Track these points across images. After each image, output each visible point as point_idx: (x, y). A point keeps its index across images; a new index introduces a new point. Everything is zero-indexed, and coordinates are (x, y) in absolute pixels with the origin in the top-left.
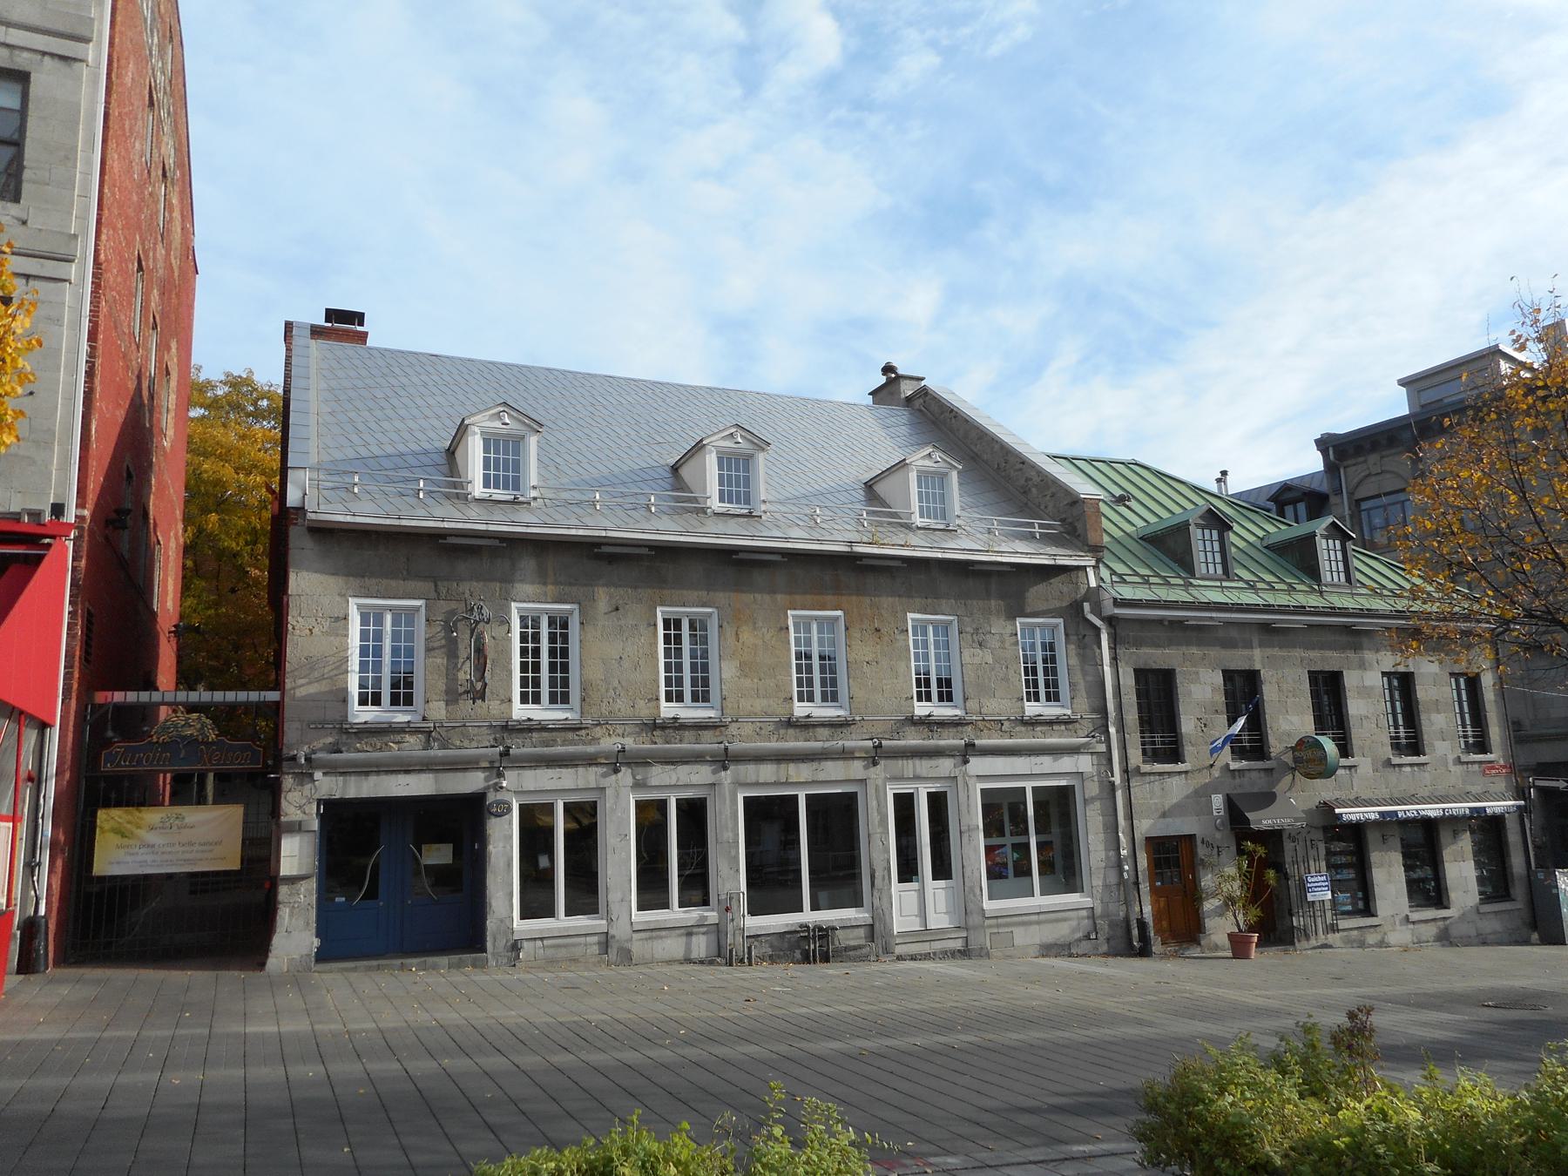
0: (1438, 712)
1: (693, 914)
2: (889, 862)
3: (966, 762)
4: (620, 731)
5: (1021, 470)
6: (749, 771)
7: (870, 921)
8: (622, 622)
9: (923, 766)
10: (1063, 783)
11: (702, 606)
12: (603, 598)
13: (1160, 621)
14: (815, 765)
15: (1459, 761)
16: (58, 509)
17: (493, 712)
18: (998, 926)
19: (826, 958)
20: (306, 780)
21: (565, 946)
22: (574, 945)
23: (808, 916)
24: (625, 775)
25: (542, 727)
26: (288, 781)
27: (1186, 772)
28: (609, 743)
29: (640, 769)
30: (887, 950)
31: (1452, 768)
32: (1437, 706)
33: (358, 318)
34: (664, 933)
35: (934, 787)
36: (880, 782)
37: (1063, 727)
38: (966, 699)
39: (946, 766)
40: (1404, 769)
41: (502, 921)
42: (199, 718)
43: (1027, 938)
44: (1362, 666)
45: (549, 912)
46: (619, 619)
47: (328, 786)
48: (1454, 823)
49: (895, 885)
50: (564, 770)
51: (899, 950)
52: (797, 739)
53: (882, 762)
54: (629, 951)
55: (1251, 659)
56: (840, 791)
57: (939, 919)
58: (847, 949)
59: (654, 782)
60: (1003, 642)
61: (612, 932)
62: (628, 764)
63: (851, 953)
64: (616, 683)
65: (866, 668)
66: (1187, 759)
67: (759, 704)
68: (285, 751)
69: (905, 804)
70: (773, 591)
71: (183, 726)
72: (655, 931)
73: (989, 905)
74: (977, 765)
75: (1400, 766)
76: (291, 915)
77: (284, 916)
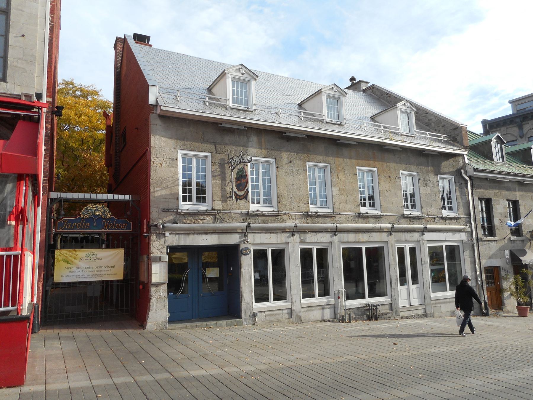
1: (324, 300)
2: (397, 277)
3: (423, 234)
4: (294, 217)
5: (425, 116)
7: (391, 302)
8: (293, 168)
9: (408, 236)
10: (455, 244)
11: (324, 163)
12: (285, 156)
13: (486, 179)
14: (369, 234)
16: (39, 96)
17: (241, 207)
18: (436, 304)
19: (376, 319)
20: (162, 236)
21: (274, 315)
22: (278, 314)
23: (368, 300)
24: (297, 237)
25: (263, 215)
26: (153, 237)
27: (496, 241)
28: (290, 224)
29: (302, 235)
30: (397, 315)
33: (148, 38)
34: (313, 308)
35: (412, 245)
36: (393, 242)
37: (456, 221)
38: (422, 208)
39: (416, 236)
41: (248, 304)
42: (103, 207)
46: (292, 167)
47: (172, 240)
49: (400, 287)
50: (272, 234)
51: (402, 314)
52: (362, 223)
53: (394, 234)
54: (300, 317)
55: (515, 195)
56: (377, 246)
57: (415, 302)
58: (383, 314)
59: (308, 240)
60: (434, 184)
61: (293, 308)
62: (298, 232)
63: (385, 316)
64: (291, 196)
65: (386, 193)
66: (497, 235)
67: (348, 207)
68: (151, 222)
69: (401, 251)
71: (95, 210)
72: (310, 307)
73: (434, 295)
74: (428, 236)
76: (157, 302)
77: (153, 302)
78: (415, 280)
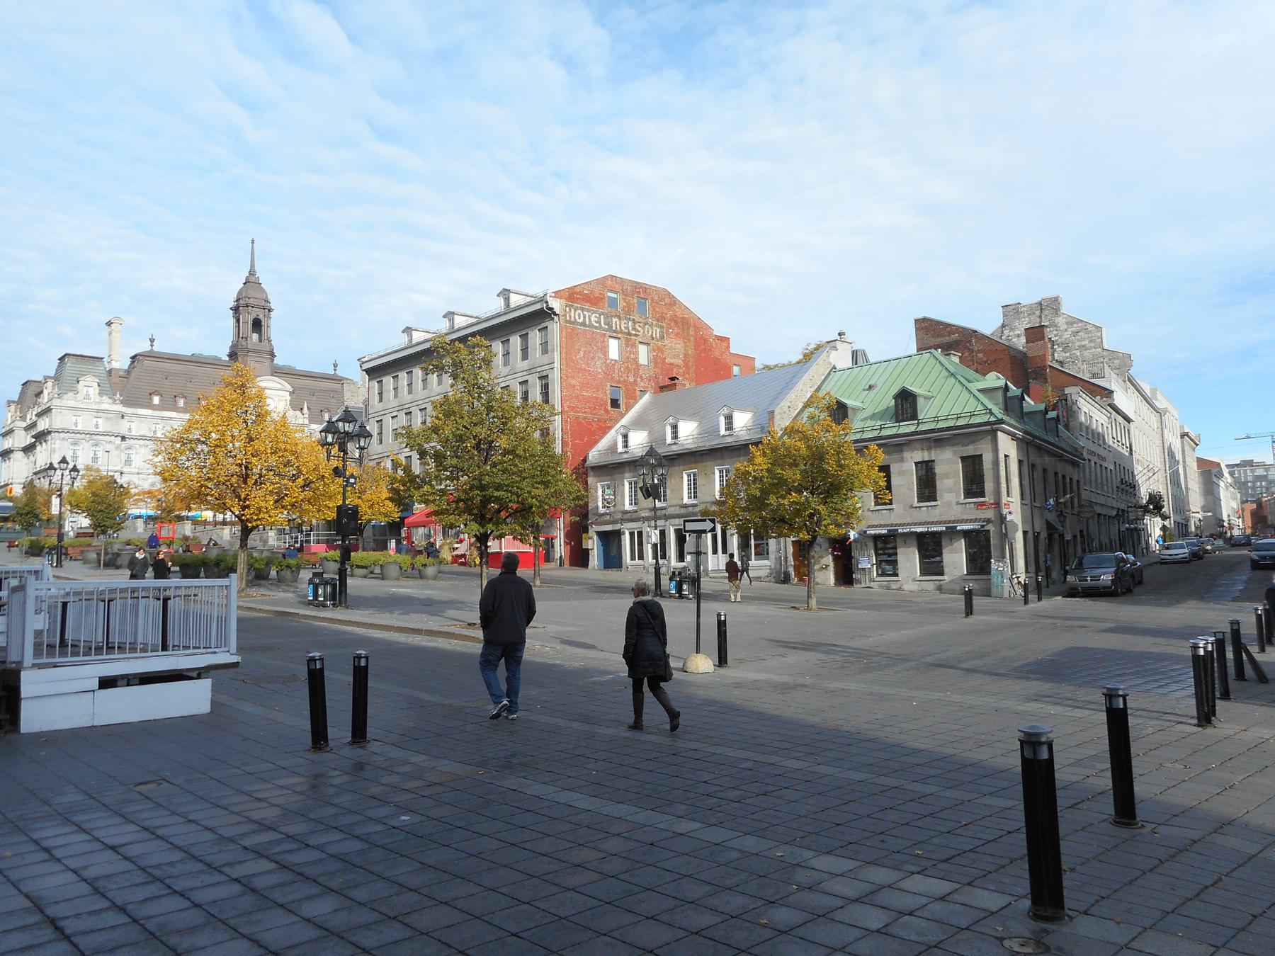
0: (948, 478)
6: (673, 521)
15: (958, 503)
26: (590, 527)
30: (707, 575)
31: (955, 507)
32: (947, 476)
40: (922, 509)
44: (902, 460)
48: (952, 533)
51: (711, 575)
70: (679, 465)
75: (920, 507)
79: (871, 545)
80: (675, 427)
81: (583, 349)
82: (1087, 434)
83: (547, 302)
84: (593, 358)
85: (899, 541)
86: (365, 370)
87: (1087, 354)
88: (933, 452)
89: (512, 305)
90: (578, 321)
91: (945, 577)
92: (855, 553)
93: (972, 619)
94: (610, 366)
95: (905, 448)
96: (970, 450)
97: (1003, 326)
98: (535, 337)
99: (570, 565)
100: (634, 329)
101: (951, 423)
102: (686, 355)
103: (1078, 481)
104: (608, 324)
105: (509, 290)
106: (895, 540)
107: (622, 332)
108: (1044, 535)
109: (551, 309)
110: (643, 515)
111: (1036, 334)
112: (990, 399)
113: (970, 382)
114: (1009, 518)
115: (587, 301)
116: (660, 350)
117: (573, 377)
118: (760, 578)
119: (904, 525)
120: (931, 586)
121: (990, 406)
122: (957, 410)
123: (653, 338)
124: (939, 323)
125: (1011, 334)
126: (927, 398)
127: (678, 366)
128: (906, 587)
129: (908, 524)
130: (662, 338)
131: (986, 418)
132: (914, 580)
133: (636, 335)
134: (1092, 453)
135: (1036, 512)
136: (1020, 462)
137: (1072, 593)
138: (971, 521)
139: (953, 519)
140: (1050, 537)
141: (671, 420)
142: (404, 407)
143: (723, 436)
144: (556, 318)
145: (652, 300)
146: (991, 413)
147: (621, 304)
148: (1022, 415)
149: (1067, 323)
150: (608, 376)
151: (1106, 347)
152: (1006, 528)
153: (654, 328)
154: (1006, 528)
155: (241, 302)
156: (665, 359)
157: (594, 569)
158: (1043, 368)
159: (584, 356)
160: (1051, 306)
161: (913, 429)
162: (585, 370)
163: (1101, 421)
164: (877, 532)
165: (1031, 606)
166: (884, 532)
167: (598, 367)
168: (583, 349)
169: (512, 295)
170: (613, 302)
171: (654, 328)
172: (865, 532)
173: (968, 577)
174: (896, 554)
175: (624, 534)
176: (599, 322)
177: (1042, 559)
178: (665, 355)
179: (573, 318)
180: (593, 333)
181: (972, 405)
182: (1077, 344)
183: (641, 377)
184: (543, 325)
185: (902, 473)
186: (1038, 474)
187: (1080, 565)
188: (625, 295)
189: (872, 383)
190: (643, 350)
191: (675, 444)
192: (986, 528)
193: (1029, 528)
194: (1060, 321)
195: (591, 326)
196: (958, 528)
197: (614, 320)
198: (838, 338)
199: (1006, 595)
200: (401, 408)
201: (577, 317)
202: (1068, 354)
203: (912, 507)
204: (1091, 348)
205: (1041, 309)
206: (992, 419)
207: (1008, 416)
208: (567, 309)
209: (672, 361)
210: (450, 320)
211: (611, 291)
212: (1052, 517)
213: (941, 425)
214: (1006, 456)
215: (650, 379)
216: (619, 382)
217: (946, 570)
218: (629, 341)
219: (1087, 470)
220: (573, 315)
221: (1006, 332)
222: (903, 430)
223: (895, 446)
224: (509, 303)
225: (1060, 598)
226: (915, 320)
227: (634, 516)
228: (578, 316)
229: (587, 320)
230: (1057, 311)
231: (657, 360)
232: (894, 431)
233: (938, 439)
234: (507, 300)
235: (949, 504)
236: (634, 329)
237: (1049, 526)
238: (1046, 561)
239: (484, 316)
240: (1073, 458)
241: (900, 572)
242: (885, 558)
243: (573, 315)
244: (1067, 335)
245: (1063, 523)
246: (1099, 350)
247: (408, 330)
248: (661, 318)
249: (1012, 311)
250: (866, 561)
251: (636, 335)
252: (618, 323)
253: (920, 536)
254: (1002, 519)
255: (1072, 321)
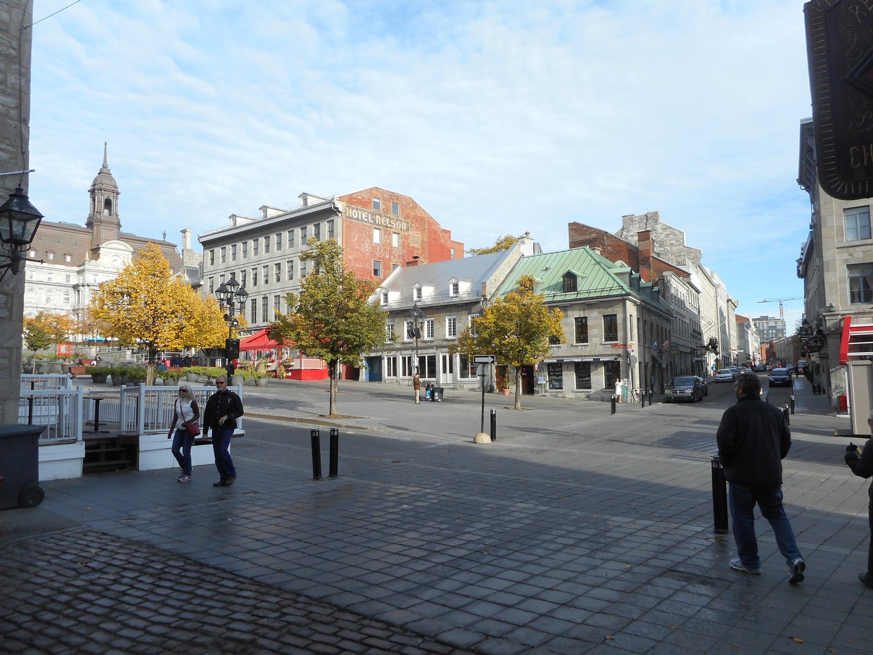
0: (595, 328)
12: (397, 320)
15: (601, 344)
31: (599, 346)
32: (594, 327)
43: (466, 387)
45: (405, 375)
48: (597, 363)
72: (403, 380)
78: (451, 371)
79: (546, 369)
80: (419, 290)
81: (357, 236)
82: (675, 300)
83: (334, 204)
84: (363, 242)
85: (564, 367)
86: (202, 242)
87: (674, 249)
88: (586, 312)
89: (309, 204)
90: (354, 217)
91: (592, 390)
92: (536, 374)
93: (615, 415)
94: (374, 247)
95: (569, 309)
96: (609, 311)
97: (623, 229)
98: (325, 226)
99: (347, 378)
100: (390, 223)
101: (598, 294)
102: (423, 242)
103: (669, 331)
104: (373, 220)
105: (307, 194)
106: (561, 367)
107: (382, 225)
108: (650, 364)
109: (337, 208)
110: (397, 347)
111: (644, 236)
112: (622, 280)
113: (609, 268)
114: (632, 354)
115: (360, 204)
116: (406, 238)
117: (350, 254)
118: (474, 389)
119: (567, 357)
120: (583, 395)
121: (622, 284)
122: (601, 286)
123: (402, 230)
124: (584, 226)
125: (628, 234)
126: (583, 278)
127: (418, 249)
128: (567, 396)
129: (570, 357)
130: (408, 230)
131: (619, 292)
132: (573, 391)
133: (391, 228)
134: (678, 313)
135: (646, 350)
136: (638, 319)
137: (668, 401)
138: (609, 355)
139: (597, 354)
140: (653, 365)
141: (417, 286)
142: (229, 269)
143: (451, 297)
144: (340, 215)
145: (402, 204)
146: (623, 289)
147: (382, 206)
148: (640, 290)
149: (662, 229)
150: (373, 254)
151: (686, 245)
152: (630, 360)
153: (403, 223)
154: (630, 360)
155: (96, 186)
156: (409, 244)
157: (362, 381)
158: (648, 258)
159: (358, 241)
160: (652, 217)
161: (574, 297)
162: (358, 249)
163: (683, 293)
164: (550, 361)
165: (646, 408)
166: (554, 361)
167: (366, 248)
168: (357, 236)
169: (309, 197)
170: (376, 206)
171: (403, 223)
172: (543, 361)
173: (606, 390)
174: (561, 375)
175: (384, 359)
176: (367, 218)
177: (649, 379)
178: (409, 241)
179: (351, 215)
180: (364, 225)
181: (611, 283)
182: (668, 242)
183: (394, 255)
184: (330, 219)
185: (567, 324)
186: (648, 327)
187: (672, 384)
188: (385, 201)
189: (547, 266)
190: (395, 237)
191: (419, 301)
192: (618, 360)
193: (642, 361)
194: (658, 227)
195: (362, 220)
196: (601, 360)
197: (378, 217)
198: (525, 236)
199: (629, 401)
200: (227, 269)
201: (353, 215)
202: (663, 249)
203: (572, 346)
204: (676, 245)
205: (647, 219)
206: (624, 292)
207: (632, 290)
208: (347, 209)
209: (414, 245)
210: (264, 211)
211: (375, 198)
212: (655, 354)
213: (592, 295)
214: (631, 316)
215: (399, 256)
216: (379, 258)
217: (592, 385)
218: (386, 231)
219: (675, 324)
220: (351, 213)
221: (625, 233)
222: (567, 298)
223: (566, 307)
224: (306, 202)
225: (661, 403)
226: (569, 224)
227: (391, 347)
228: (354, 214)
229: (360, 216)
230: (656, 221)
231: (404, 244)
232: (562, 298)
233: (590, 304)
234: (305, 201)
235: (595, 345)
236: (390, 223)
237: (653, 359)
238: (651, 381)
239: (289, 211)
240: (666, 316)
241: (563, 386)
242: (555, 377)
243: (351, 213)
244: (662, 237)
245: (661, 357)
246: (682, 247)
247: (233, 217)
248: (407, 217)
249: (628, 220)
250: (543, 379)
251: (391, 228)
252: (380, 219)
253: (577, 364)
254: (627, 355)
255: (666, 228)
